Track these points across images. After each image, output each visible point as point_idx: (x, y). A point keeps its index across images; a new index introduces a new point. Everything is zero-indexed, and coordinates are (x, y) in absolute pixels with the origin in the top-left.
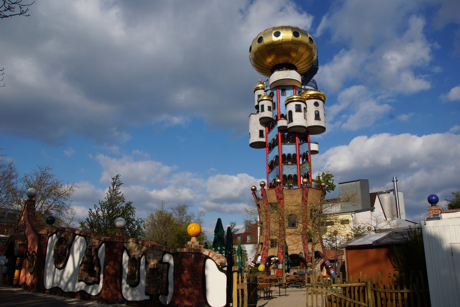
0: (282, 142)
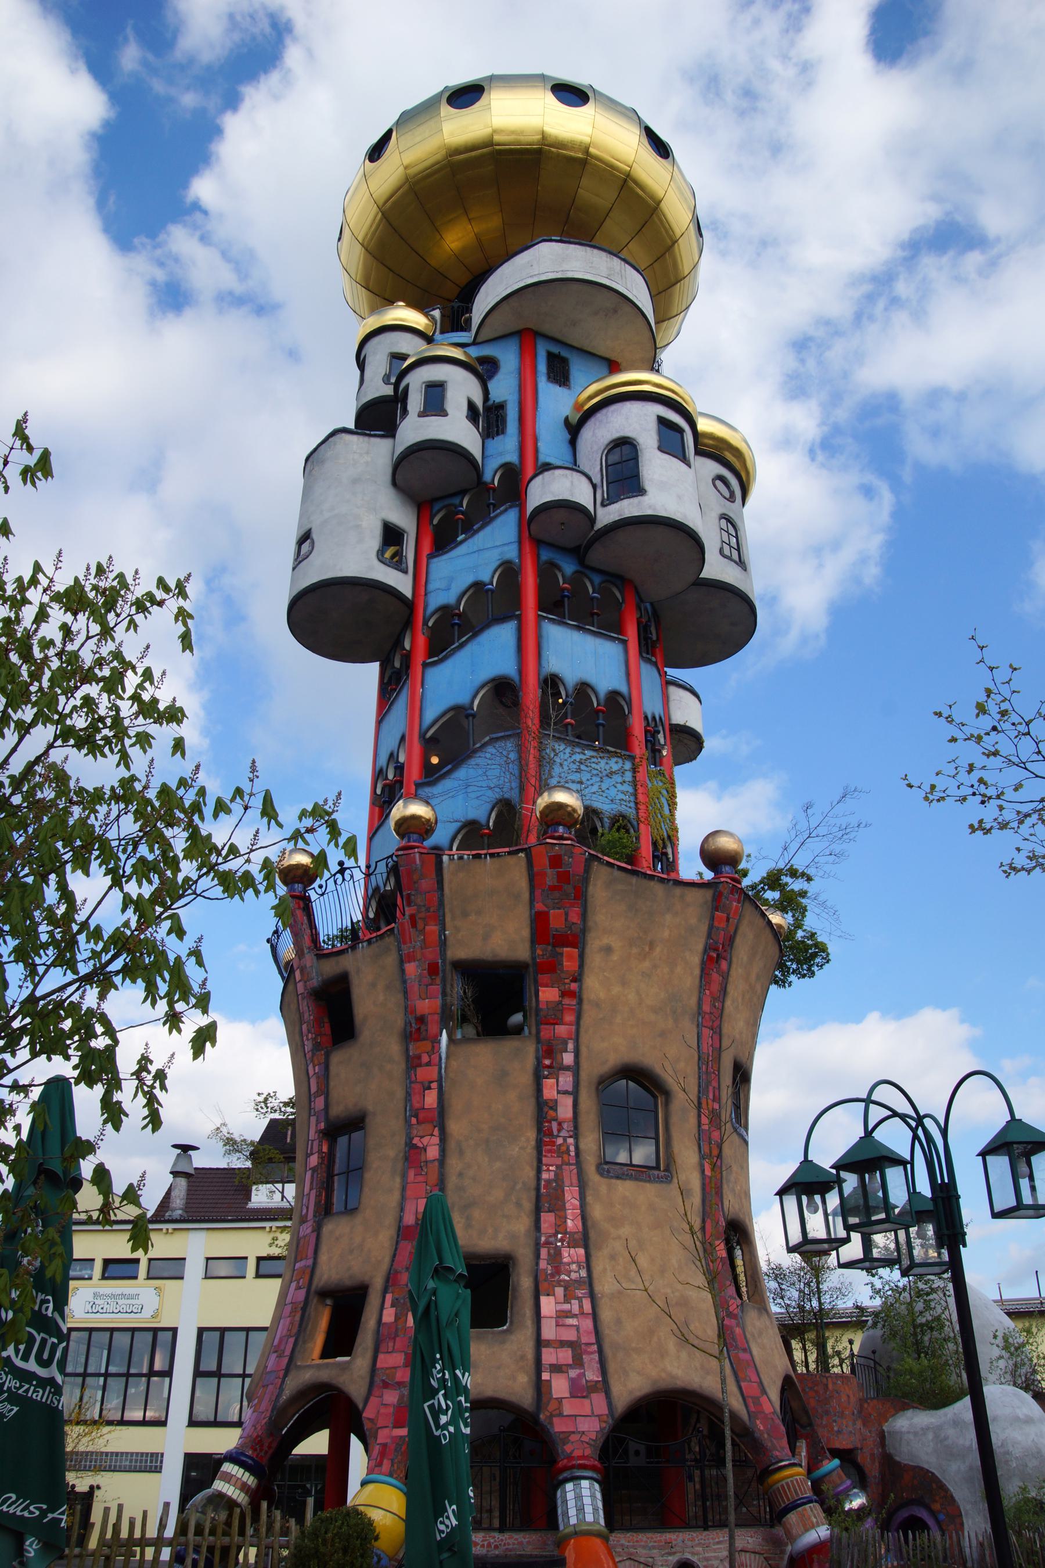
0: (542, 606)
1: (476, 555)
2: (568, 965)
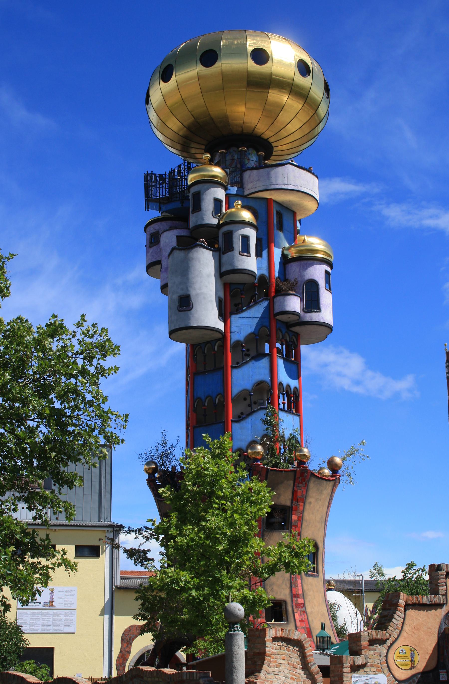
1: (250, 319)
2: (301, 508)
